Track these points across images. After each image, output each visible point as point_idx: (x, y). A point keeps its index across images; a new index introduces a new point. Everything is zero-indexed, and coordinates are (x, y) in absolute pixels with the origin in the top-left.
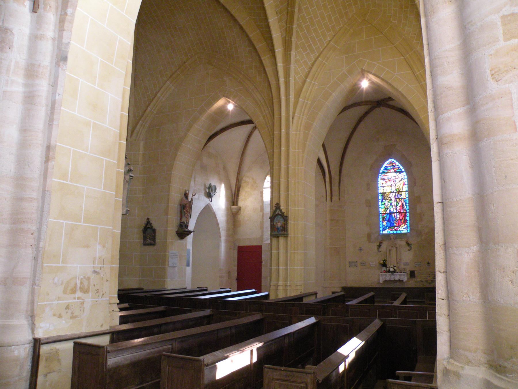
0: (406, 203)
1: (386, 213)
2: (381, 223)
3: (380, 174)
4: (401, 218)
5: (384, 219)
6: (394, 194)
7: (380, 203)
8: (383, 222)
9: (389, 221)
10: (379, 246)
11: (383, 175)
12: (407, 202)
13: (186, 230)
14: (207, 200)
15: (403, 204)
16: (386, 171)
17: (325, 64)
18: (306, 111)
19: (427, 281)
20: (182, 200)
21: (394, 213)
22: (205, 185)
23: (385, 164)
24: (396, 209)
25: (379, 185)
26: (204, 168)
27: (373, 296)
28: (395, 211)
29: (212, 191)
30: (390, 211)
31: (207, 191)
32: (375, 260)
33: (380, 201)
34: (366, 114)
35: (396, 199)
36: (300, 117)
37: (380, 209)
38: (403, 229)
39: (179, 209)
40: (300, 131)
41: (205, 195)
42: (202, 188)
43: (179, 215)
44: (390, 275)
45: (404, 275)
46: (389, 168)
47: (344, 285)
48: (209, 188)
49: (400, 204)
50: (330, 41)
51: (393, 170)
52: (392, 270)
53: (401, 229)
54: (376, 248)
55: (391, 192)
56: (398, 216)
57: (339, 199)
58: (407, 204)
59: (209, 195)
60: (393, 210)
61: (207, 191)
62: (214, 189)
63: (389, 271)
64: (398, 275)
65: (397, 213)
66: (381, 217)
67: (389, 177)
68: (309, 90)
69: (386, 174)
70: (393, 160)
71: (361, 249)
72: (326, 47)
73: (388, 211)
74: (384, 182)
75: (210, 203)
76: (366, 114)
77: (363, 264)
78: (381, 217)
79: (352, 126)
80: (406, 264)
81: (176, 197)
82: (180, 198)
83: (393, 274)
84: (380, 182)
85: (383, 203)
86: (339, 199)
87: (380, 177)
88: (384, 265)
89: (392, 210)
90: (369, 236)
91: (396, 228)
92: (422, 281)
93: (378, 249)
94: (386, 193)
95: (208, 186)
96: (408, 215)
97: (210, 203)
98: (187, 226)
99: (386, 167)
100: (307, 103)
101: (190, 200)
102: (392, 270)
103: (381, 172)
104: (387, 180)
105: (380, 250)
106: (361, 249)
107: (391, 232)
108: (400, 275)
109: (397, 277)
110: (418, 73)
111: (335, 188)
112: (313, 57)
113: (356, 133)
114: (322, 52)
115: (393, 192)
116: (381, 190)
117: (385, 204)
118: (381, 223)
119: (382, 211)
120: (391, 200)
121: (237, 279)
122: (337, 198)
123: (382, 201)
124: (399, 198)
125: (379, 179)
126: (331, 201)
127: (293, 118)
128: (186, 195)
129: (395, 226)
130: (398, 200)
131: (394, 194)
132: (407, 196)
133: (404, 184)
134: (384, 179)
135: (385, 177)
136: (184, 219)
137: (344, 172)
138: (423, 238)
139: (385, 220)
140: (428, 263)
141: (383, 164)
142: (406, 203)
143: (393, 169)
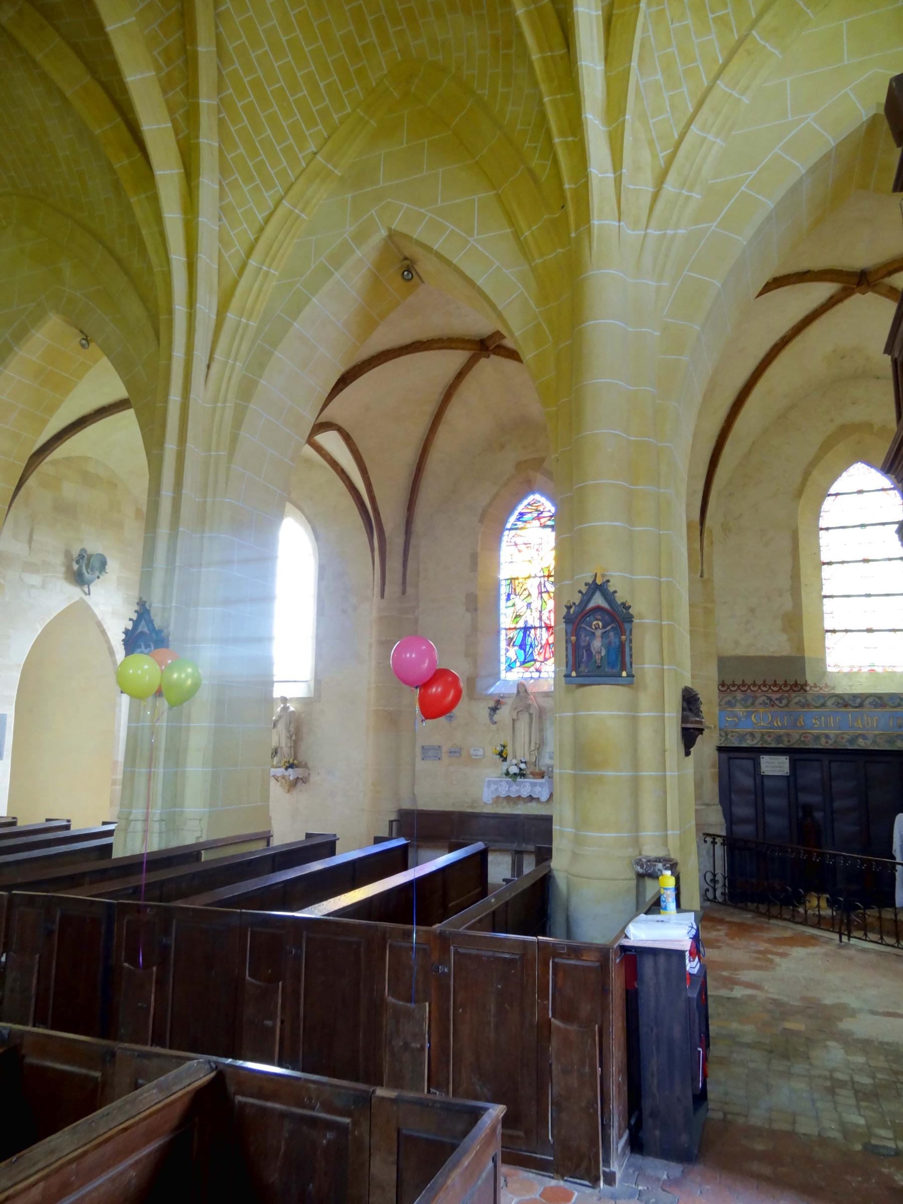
1: (515, 628)
3: (506, 533)
5: (510, 641)
6: (537, 580)
8: (507, 650)
9: (522, 646)
14: (74, 593)
17: (298, 217)
18: (244, 348)
21: (535, 628)
22: (68, 554)
23: (520, 508)
24: (540, 619)
27: (405, 848)
28: (537, 625)
30: (526, 622)
31: (75, 567)
34: (460, 376)
35: (541, 593)
36: (226, 363)
40: (225, 401)
41: (66, 579)
42: (58, 561)
44: (508, 782)
45: (541, 785)
46: (526, 517)
47: (407, 806)
50: (315, 154)
51: (537, 523)
54: (486, 713)
55: (529, 577)
57: (404, 592)
61: (75, 567)
64: (527, 785)
65: (541, 627)
66: (503, 637)
67: (526, 540)
69: (518, 532)
70: (537, 497)
72: (304, 170)
73: (521, 624)
74: (514, 549)
75: (86, 598)
76: (460, 376)
79: (430, 409)
84: (506, 551)
85: (510, 603)
86: (404, 592)
91: (538, 664)
93: (491, 716)
95: (75, 554)
97: (86, 598)
100: (247, 325)
103: (508, 526)
104: (523, 547)
105: (496, 718)
107: (528, 675)
108: (533, 785)
111: (394, 563)
112: (269, 197)
113: (442, 429)
114: (292, 185)
115: (536, 576)
116: (504, 573)
117: (514, 605)
118: (503, 652)
119: (506, 620)
120: (529, 595)
122: (398, 589)
125: (504, 544)
126: (382, 596)
129: (535, 660)
135: (518, 540)
137: (419, 524)
139: (513, 645)
143: (538, 518)
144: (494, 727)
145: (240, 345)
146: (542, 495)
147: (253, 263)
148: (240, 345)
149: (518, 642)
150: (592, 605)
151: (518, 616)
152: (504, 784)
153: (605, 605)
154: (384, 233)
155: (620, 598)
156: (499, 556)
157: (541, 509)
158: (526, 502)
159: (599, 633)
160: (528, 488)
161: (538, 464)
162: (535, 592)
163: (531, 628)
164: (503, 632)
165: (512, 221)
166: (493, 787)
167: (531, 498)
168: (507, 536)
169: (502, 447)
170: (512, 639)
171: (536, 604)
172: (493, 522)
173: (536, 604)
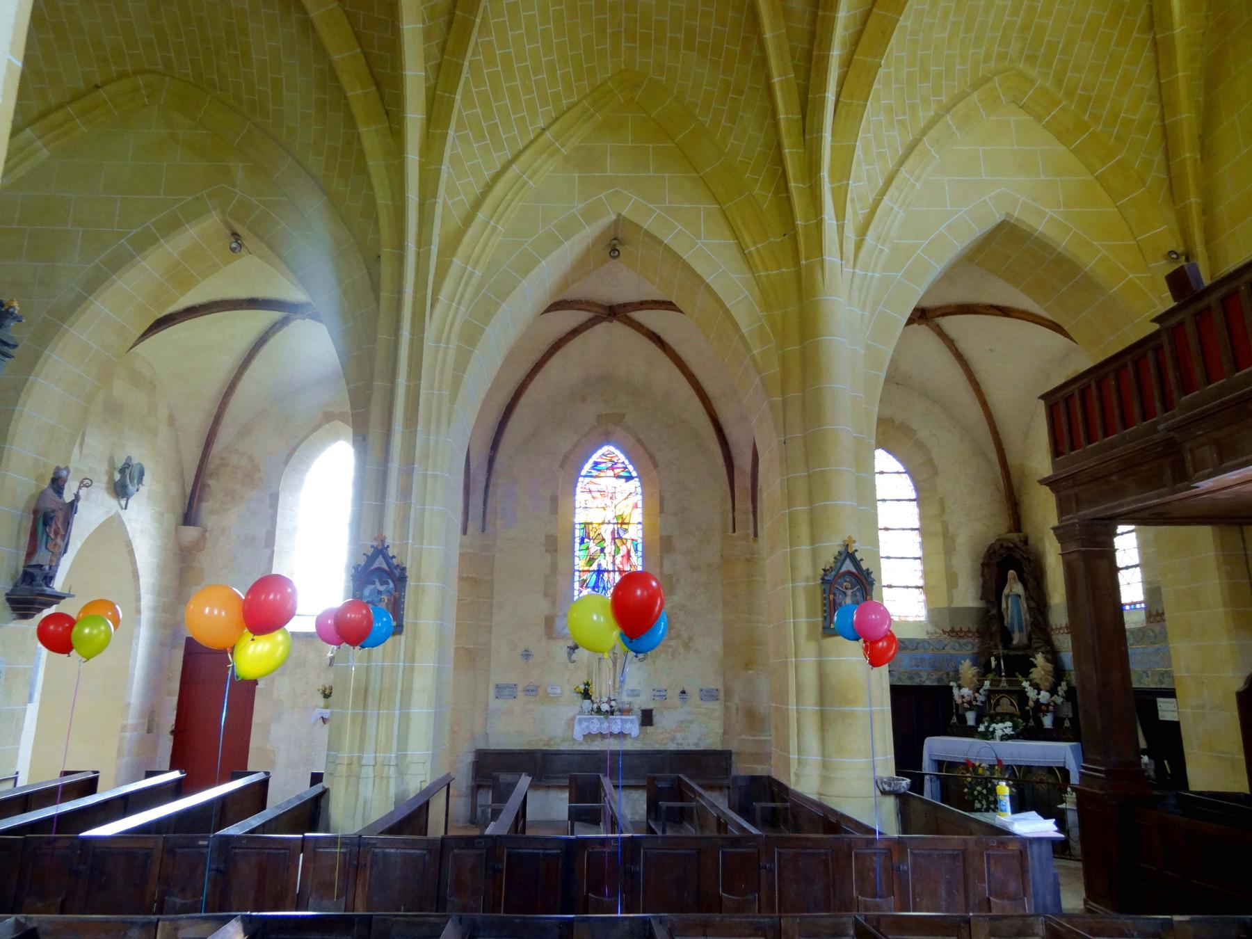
0: (636, 551)
5: (583, 583)
6: (611, 527)
7: (577, 546)
11: (588, 479)
12: (640, 548)
13: (48, 591)
15: (629, 552)
16: (594, 473)
20: (42, 494)
21: (608, 571)
24: (614, 563)
25: (577, 505)
26: (114, 411)
28: (610, 568)
29: (131, 480)
30: (599, 565)
33: (577, 541)
34: (575, 332)
35: (614, 539)
37: (577, 560)
39: (28, 524)
41: (107, 489)
42: (103, 468)
43: (25, 539)
45: (632, 722)
46: (603, 466)
47: (482, 746)
48: (122, 471)
49: (623, 550)
51: (610, 473)
52: (605, 707)
54: (563, 653)
57: (484, 530)
58: (640, 554)
59: (120, 490)
60: (606, 563)
61: (117, 477)
62: (136, 475)
63: (599, 711)
64: (619, 722)
66: (576, 578)
67: (602, 488)
68: (482, 241)
70: (612, 448)
73: (595, 567)
74: (588, 496)
75: (122, 512)
76: (575, 332)
79: (535, 357)
81: (22, 482)
82: (33, 491)
84: (580, 497)
85: (584, 547)
86: (484, 530)
87: (579, 484)
88: (586, 695)
89: (604, 566)
93: (570, 655)
95: (119, 465)
97: (122, 512)
98: (49, 579)
99: (596, 464)
101: (68, 497)
102: (605, 707)
103: (583, 473)
104: (597, 495)
105: (574, 657)
110: (753, 249)
112: (498, 160)
113: (539, 377)
115: (609, 523)
116: (580, 517)
118: (576, 593)
119: (580, 563)
121: (173, 732)
123: (582, 542)
125: (578, 490)
126: (465, 531)
127: (432, 305)
128: (57, 483)
131: (611, 527)
132: (640, 534)
133: (636, 506)
135: (593, 487)
136: (42, 557)
137: (497, 466)
140: (683, 692)
141: (590, 457)
142: (636, 551)
143: (612, 468)
144: (571, 666)
145: (465, 290)
146: (617, 448)
147: (481, 216)
148: (465, 290)
149: (592, 584)
150: (844, 569)
151: (591, 560)
152: (595, 721)
153: (853, 570)
154: (613, 217)
155: (864, 566)
156: (574, 501)
157: (615, 460)
158: (600, 452)
159: (849, 592)
160: (607, 439)
161: (618, 419)
162: (608, 537)
163: (605, 571)
164: (577, 574)
165: (735, 234)
166: (585, 724)
167: (605, 449)
168: (582, 483)
169: (584, 399)
170: (585, 581)
171: (610, 548)
172: (569, 468)
173: (610, 548)
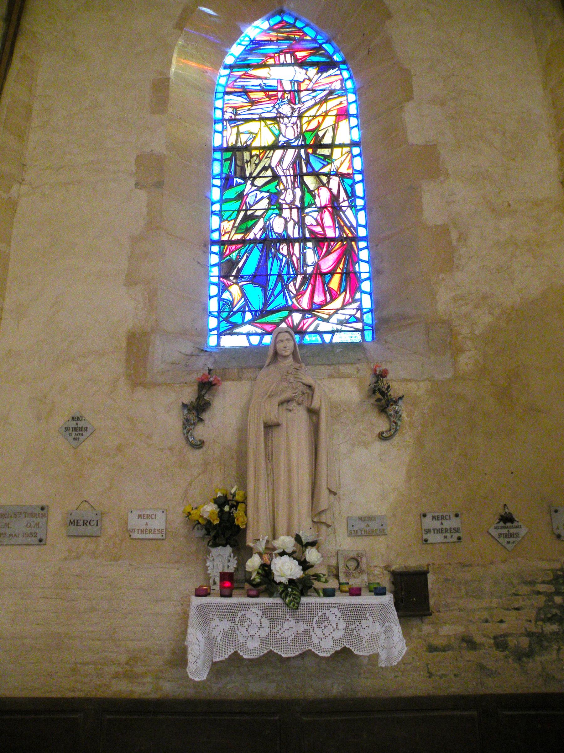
0: (352, 196)
2: (214, 290)
4: (327, 264)
5: (229, 269)
6: (291, 154)
7: (216, 194)
8: (224, 288)
10: (198, 408)
12: (359, 190)
15: (334, 198)
19: (500, 643)
21: (289, 241)
24: (301, 223)
28: (294, 232)
30: (268, 228)
32: (161, 495)
35: (299, 176)
38: (341, 322)
44: (266, 611)
49: (324, 197)
51: (289, 58)
52: (286, 569)
53: (323, 327)
54: (173, 421)
55: (274, 147)
56: (311, 257)
58: (360, 203)
63: (266, 583)
64: (334, 615)
65: (303, 240)
69: (252, 72)
71: (76, 429)
73: (256, 232)
74: (238, 100)
77: (81, 525)
78: (214, 259)
80: (366, 526)
83: (294, 607)
85: (231, 193)
88: (225, 530)
90: (136, 347)
92: (469, 643)
93: (187, 426)
94: (248, 148)
96: (364, 255)
102: (286, 569)
103: (229, 60)
105: (200, 432)
106: (76, 429)
108: (354, 615)
109: (324, 629)
115: (287, 146)
117: (241, 196)
123: (227, 183)
124: (316, 174)
130: (310, 181)
131: (291, 154)
132: (358, 164)
133: (343, 114)
134: (245, 92)
135: (251, 83)
138: (466, 361)
142: (352, 196)
